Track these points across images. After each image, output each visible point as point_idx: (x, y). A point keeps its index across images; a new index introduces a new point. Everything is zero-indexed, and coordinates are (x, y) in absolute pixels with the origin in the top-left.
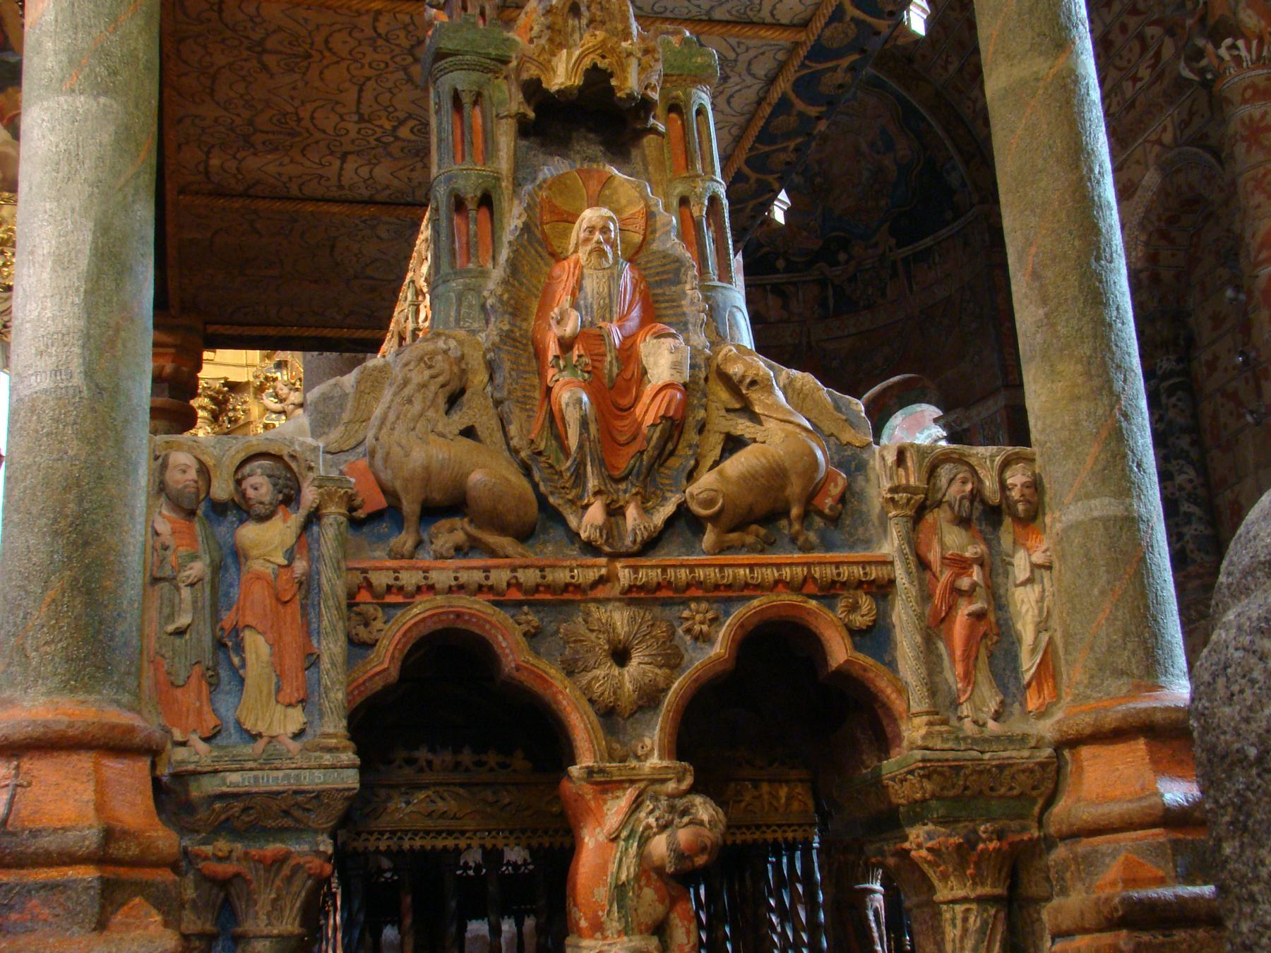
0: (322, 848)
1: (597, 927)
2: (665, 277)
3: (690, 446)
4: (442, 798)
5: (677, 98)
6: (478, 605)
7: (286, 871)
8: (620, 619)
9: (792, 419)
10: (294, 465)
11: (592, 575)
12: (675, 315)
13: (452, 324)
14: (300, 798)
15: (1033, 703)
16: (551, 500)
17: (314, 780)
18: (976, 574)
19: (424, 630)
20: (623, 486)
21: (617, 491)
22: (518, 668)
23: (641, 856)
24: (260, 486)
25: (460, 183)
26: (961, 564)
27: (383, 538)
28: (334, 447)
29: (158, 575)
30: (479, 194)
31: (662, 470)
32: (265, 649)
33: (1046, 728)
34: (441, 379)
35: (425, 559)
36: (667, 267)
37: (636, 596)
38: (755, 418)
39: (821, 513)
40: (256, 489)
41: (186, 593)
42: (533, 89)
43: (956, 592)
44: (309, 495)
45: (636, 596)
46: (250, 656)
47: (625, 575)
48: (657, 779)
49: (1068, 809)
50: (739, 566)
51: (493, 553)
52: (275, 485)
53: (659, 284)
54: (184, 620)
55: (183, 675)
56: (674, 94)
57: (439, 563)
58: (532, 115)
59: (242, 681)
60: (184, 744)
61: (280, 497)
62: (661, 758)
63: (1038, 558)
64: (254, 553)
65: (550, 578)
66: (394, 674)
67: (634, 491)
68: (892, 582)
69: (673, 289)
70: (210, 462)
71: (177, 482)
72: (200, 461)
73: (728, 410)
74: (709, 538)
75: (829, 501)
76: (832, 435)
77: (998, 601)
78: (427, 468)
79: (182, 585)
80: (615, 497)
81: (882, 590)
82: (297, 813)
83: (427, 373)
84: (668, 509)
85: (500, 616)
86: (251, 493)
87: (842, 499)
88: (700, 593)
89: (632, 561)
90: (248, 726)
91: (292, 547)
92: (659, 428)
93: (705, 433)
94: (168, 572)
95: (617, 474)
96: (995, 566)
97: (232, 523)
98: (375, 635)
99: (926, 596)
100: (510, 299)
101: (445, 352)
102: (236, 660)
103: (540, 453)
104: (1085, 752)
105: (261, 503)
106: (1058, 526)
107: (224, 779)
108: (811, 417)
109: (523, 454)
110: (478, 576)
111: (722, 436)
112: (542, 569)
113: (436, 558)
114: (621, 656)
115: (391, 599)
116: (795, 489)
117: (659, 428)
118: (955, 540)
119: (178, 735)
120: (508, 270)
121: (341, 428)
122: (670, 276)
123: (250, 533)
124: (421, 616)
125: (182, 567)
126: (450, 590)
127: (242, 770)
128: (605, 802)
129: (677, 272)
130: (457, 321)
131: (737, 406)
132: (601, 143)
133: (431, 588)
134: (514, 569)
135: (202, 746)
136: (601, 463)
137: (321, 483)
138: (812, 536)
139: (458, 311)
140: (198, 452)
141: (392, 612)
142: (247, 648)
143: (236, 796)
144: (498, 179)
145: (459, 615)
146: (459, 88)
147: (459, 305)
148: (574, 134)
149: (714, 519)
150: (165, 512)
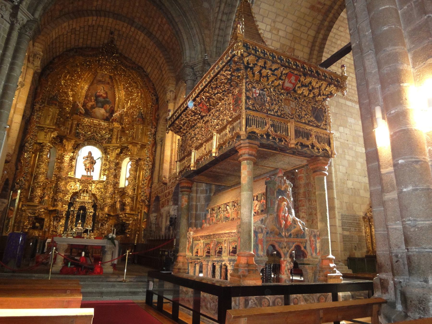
24: (260, 230)
26: (313, 241)
50: (295, 240)
77: (316, 245)
81: (306, 242)
84: (289, 234)
96: (316, 241)
118: (313, 239)
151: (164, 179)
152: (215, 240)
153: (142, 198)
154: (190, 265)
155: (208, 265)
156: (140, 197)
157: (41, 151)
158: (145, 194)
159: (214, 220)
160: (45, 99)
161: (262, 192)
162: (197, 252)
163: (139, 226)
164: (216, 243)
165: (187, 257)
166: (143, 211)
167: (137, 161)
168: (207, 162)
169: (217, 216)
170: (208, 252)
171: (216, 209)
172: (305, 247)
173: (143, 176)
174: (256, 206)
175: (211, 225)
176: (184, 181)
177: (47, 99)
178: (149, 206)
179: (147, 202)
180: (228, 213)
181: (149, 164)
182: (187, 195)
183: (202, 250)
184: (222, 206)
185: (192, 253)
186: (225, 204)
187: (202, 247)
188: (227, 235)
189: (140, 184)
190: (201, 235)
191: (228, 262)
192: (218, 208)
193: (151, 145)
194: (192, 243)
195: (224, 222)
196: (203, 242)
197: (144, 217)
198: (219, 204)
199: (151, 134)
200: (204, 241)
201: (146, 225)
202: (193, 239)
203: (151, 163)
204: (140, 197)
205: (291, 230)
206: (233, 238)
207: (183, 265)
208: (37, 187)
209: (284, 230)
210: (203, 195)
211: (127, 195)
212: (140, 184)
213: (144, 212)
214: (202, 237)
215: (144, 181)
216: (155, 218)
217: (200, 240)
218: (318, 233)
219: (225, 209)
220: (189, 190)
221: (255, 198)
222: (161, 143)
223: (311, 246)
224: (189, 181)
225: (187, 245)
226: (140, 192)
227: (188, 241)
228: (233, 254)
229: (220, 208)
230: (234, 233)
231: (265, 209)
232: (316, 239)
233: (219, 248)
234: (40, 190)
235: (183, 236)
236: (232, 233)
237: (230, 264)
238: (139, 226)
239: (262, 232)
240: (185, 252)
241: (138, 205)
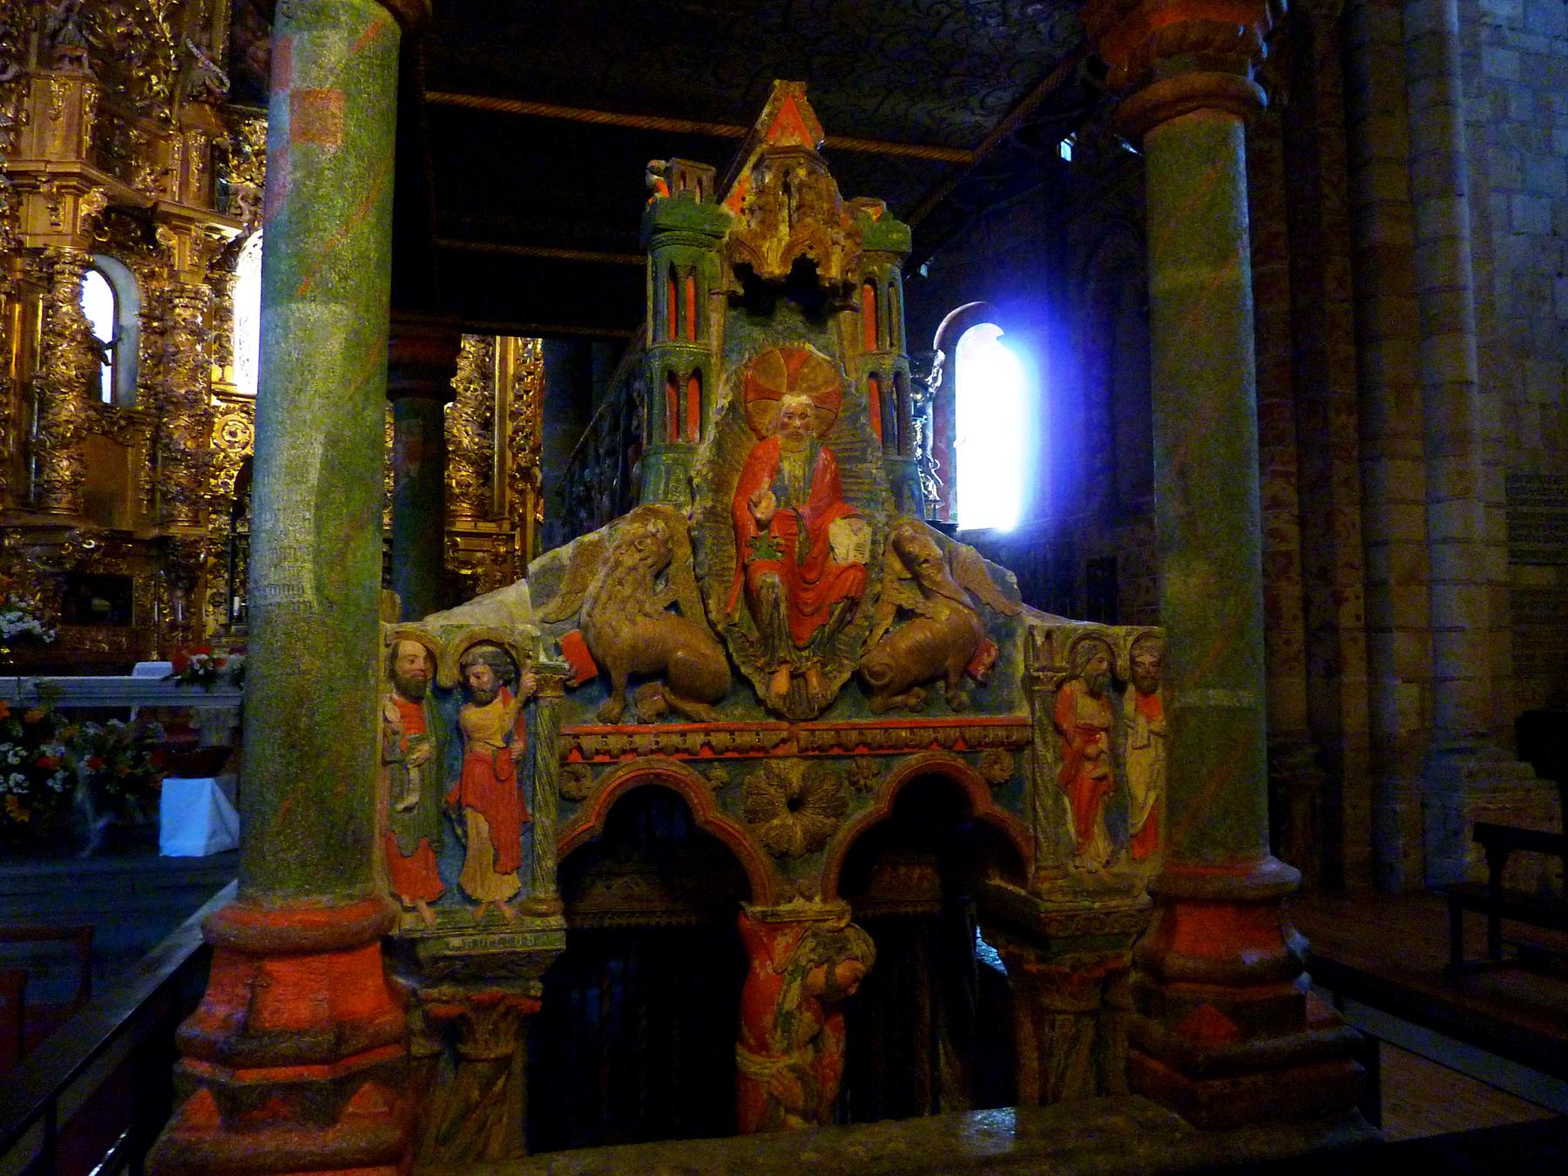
0: (533, 993)
2: (852, 454)
3: (866, 618)
4: (638, 885)
5: (873, 273)
6: (672, 767)
7: (502, 1008)
9: (956, 597)
10: (513, 653)
11: (775, 738)
12: (859, 491)
13: (661, 497)
14: (512, 957)
16: (743, 669)
17: (524, 943)
18: (1103, 741)
19: (629, 787)
20: (805, 653)
21: (800, 658)
22: (707, 822)
23: (804, 987)
24: (483, 675)
26: (1090, 732)
27: (592, 701)
28: (552, 617)
29: (388, 759)
30: (690, 371)
31: (840, 636)
32: (484, 827)
34: (649, 561)
35: (630, 724)
36: (857, 445)
39: (974, 678)
40: (478, 678)
41: (414, 774)
42: (744, 272)
44: (529, 680)
46: (472, 832)
50: (902, 726)
51: (689, 718)
52: (496, 672)
53: (849, 459)
54: (412, 799)
55: (411, 847)
56: (871, 268)
57: (643, 728)
58: (741, 291)
59: (465, 848)
60: (413, 909)
61: (501, 682)
62: (824, 901)
65: (738, 741)
66: (599, 828)
67: (815, 659)
69: (860, 466)
70: (437, 652)
71: (405, 672)
72: (428, 649)
73: (900, 579)
75: (982, 669)
76: (988, 604)
77: (1117, 760)
78: (634, 648)
79: (409, 766)
80: (798, 665)
83: (637, 556)
86: (473, 680)
87: (993, 666)
88: (866, 751)
89: (810, 725)
90: (469, 891)
91: (511, 731)
92: (841, 605)
93: (880, 603)
94: (398, 756)
95: (801, 644)
96: (1117, 729)
97: (457, 700)
98: (584, 792)
100: (715, 476)
101: (654, 535)
102: (459, 831)
103: (735, 625)
105: (484, 691)
107: (447, 944)
108: (970, 586)
109: (719, 628)
111: (894, 608)
112: (732, 733)
113: (639, 723)
115: (598, 759)
117: (841, 605)
119: (407, 902)
120: (714, 450)
121: (558, 600)
122: (857, 454)
123: (472, 715)
124: (625, 777)
125: (411, 750)
127: (462, 935)
128: (775, 939)
129: (864, 450)
130: (666, 493)
131: (909, 576)
132: (803, 312)
133: (634, 751)
134: (707, 734)
135: (428, 913)
137: (539, 669)
138: (964, 697)
139: (667, 484)
140: (425, 641)
141: (600, 769)
142: (469, 823)
144: (708, 356)
145: (658, 776)
146: (676, 262)
147: (668, 479)
148: (778, 304)
150: (395, 696)
157: (50, 282)
160: (27, 42)
166: (530, 519)
177: (34, 37)
197: (535, 547)
208: (54, 448)
211: (453, 451)
215: (520, 379)
234: (69, 458)
241: (508, 490)
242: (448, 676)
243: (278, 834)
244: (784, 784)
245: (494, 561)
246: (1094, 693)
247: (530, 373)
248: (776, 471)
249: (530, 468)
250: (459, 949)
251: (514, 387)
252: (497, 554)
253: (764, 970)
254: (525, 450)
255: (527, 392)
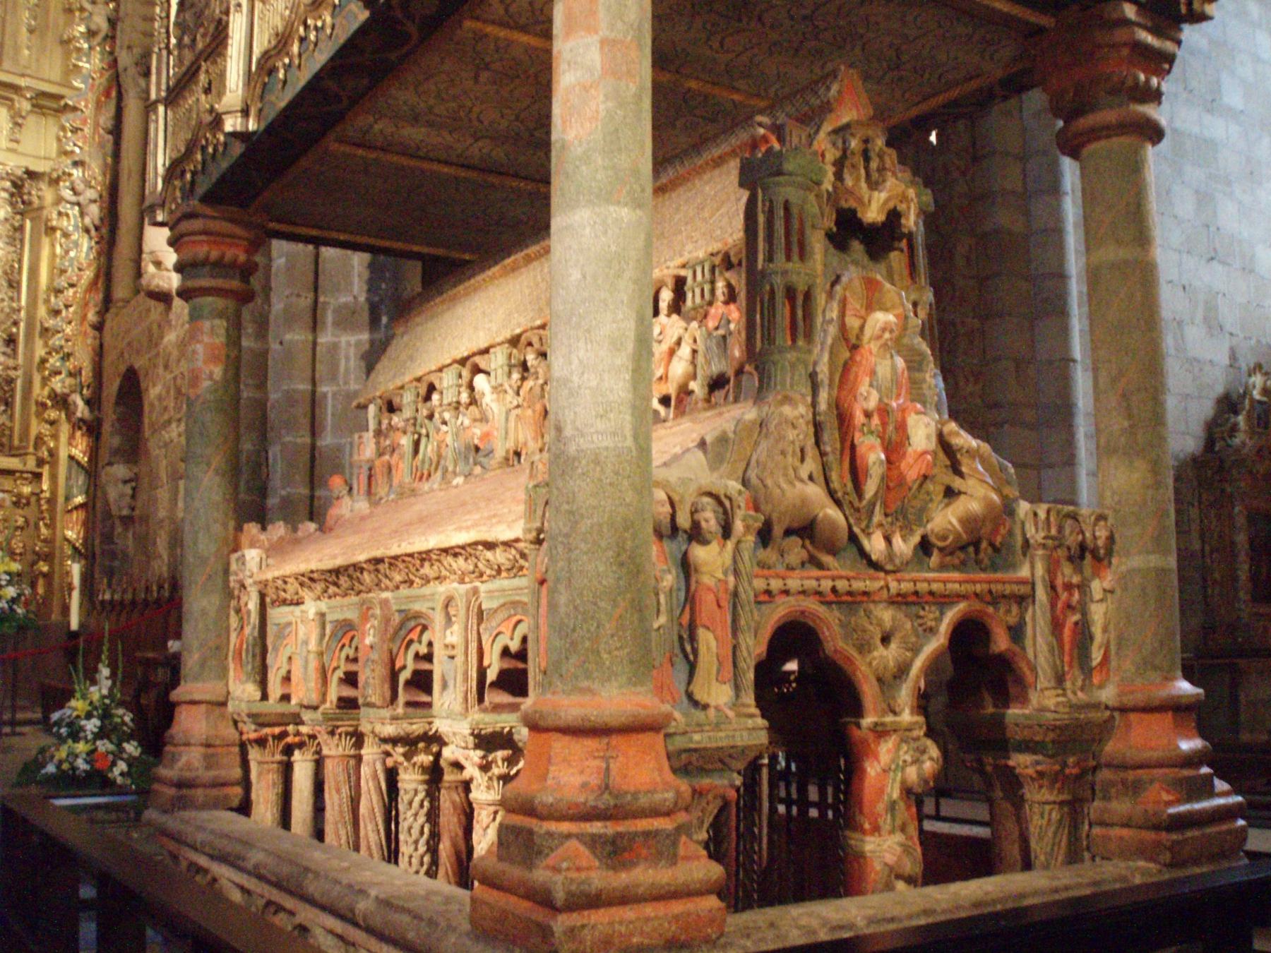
1: (876, 829)
6: (812, 605)
8: (886, 615)
10: (727, 503)
15: (1096, 681)
17: (742, 739)
22: (836, 651)
24: (710, 520)
25: (794, 278)
26: (1069, 587)
32: (713, 644)
33: (1108, 694)
37: (899, 601)
38: (960, 474)
43: (1069, 606)
45: (899, 601)
46: (702, 649)
47: (894, 586)
48: (909, 729)
49: (1111, 748)
50: (952, 581)
58: (835, 229)
62: (912, 713)
63: (1107, 585)
64: (704, 569)
68: (1033, 596)
70: (676, 498)
74: (935, 559)
77: (1084, 614)
81: (1023, 600)
82: (727, 760)
84: (916, 539)
85: (822, 610)
86: (703, 524)
96: (1083, 587)
99: (1053, 605)
102: (688, 648)
104: (1133, 717)
106: (1123, 568)
107: (691, 740)
110: (814, 583)
114: (886, 640)
116: (986, 530)
118: (1067, 573)
123: (700, 553)
126: (800, 593)
130: (792, 386)
133: (786, 592)
136: (885, 505)
139: (792, 378)
143: (695, 750)
149: (941, 550)
151: (151, 269)
152: (385, 603)
153: (58, 384)
154: (254, 754)
155: (359, 759)
156: (45, 381)
158: (70, 365)
159: (403, 473)
161: (716, 246)
162: (287, 679)
163: (44, 531)
164: (397, 618)
165: (231, 707)
166: (63, 454)
167: (14, 184)
168: (321, 58)
169: (417, 444)
170: (351, 679)
171: (408, 398)
172: (1016, 632)
173: (52, 267)
174: (672, 352)
175: (379, 510)
176: (197, 224)
178: (93, 429)
179: (80, 403)
180: (483, 419)
181: (81, 199)
182: (221, 315)
183: (313, 664)
184: (447, 381)
185: (263, 684)
186: (463, 362)
187: (313, 646)
188: (460, 564)
189: (42, 311)
190: (303, 567)
191: (476, 755)
192: (423, 390)
193: (91, 97)
194: (254, 618)
195: (459, 480)
196: (322, 615)
197: (69, 488)
198: (424, 365)
199: (91, 34)
200: (323, 605)
201: (85, 524)
202: (262, 596)
203: (91, 194)
204: (45, 381)
205: (922, 516)
206: (503, 583)
207: (210, 761)
209: (878, 517)
210: (353, 339)
212: (42, 311)
213: (71, 458)
214: (308, 579)
216: (128, 490)
217: (299, 603)
218: (1102, 533)
219: (464, 397)
220: (235, 284)
221: (666, 296)
222: (142, 82)
223: (1056, 626)
224: (226, 227)
225: (233, 636)
226: (40, 352)
227: (238, 611)
228: (504, 698)
229: (431, 388)
230: (507, 544)
231: (739, 372)
232: (1088, 571)
233: (417, 656)
235: (201, 579)
236: (490, 546)
237: (485, 768)
238: (44, 530)
239: (727, 531)
240: (223, 673)
242: (684, 521)
243: (612, 636)
244: (880, 623)
245: (16, 504)
246: (1070, 559)
247: (72, 285)
248: (873, 373)
249: (68, 395)
250: (698, 742)
251: (47, 301)
252: (19, 496)
253: (872, 770)
254: (60, 373)
255: (67, 307)
